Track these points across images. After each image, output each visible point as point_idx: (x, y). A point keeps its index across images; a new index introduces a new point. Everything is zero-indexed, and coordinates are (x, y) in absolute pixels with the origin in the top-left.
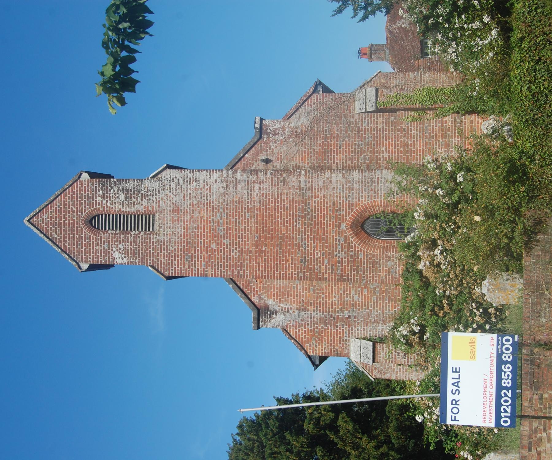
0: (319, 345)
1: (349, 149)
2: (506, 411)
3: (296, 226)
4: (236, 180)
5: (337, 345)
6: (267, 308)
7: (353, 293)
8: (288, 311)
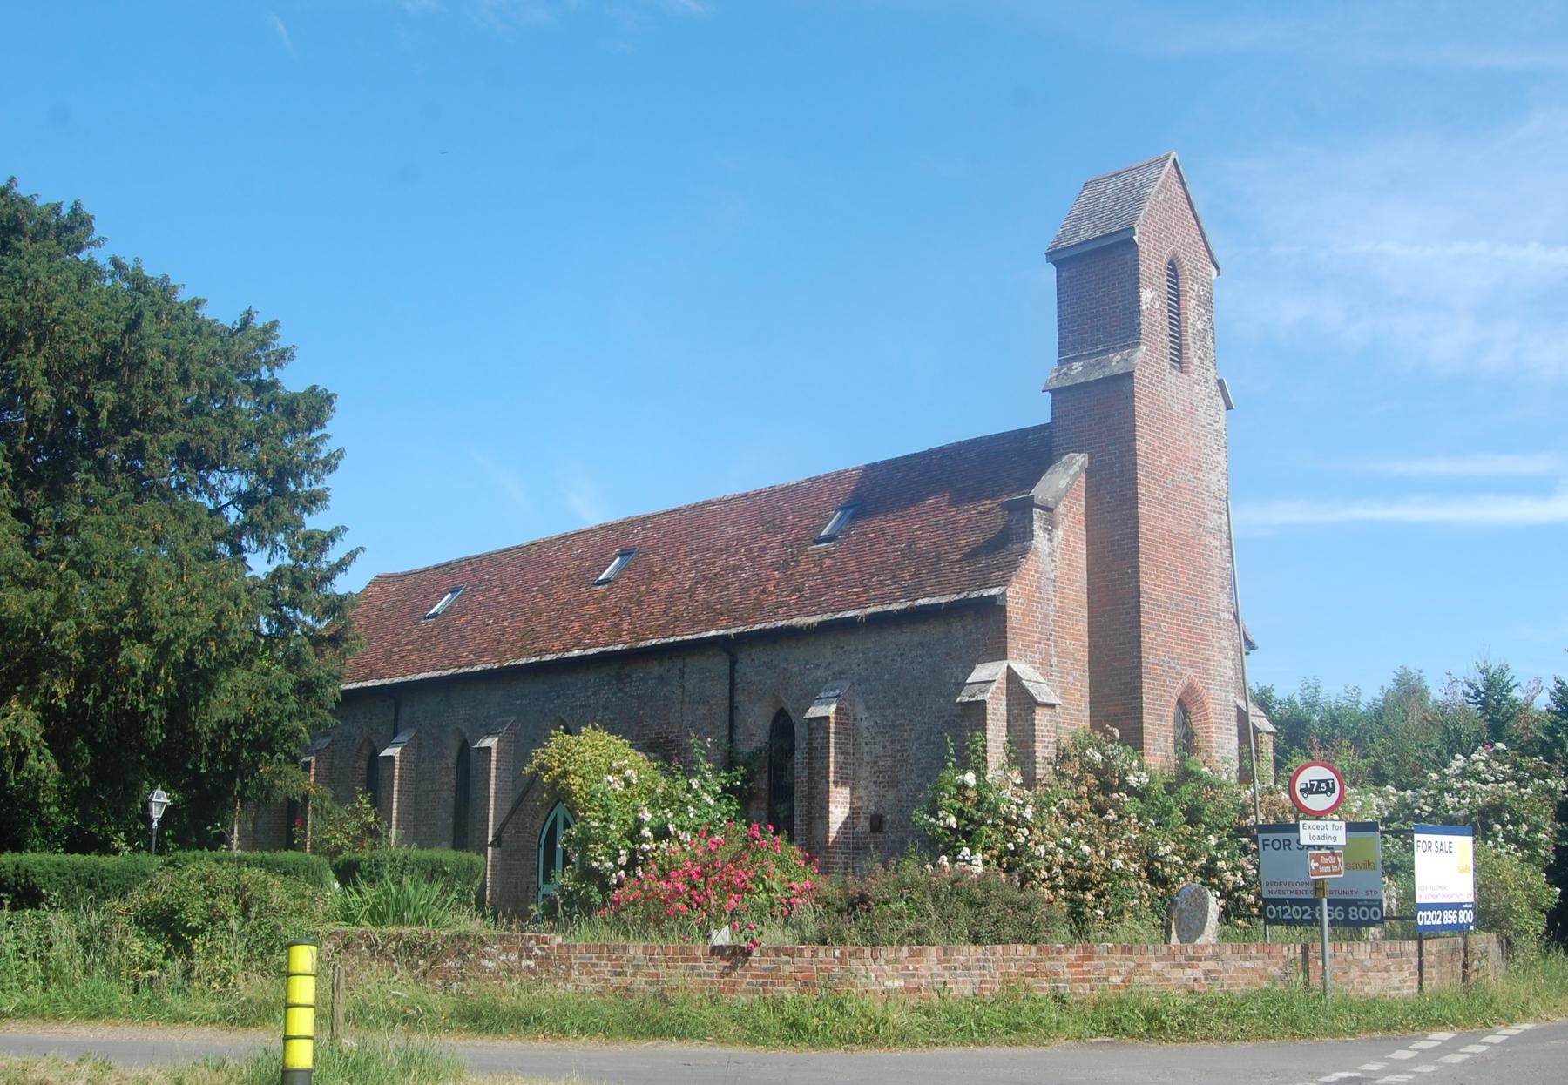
7: (1077, 674)
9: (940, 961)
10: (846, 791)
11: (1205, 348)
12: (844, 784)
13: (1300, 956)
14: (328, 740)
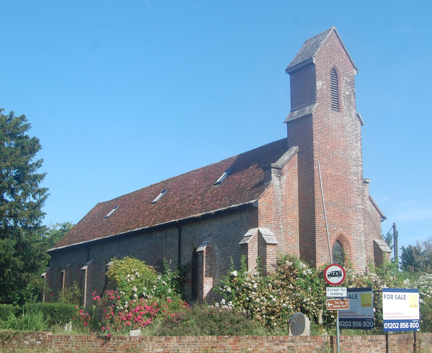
0: (264, 207)
2: (390, 325)
6: (282, 174)
7: (292, 232)
8: (281, 188)
9: (178, 342)
10: (211, 279)
11: (350, 103)
12: (210, 276)
13: (329, 341)
14: (70, 264)
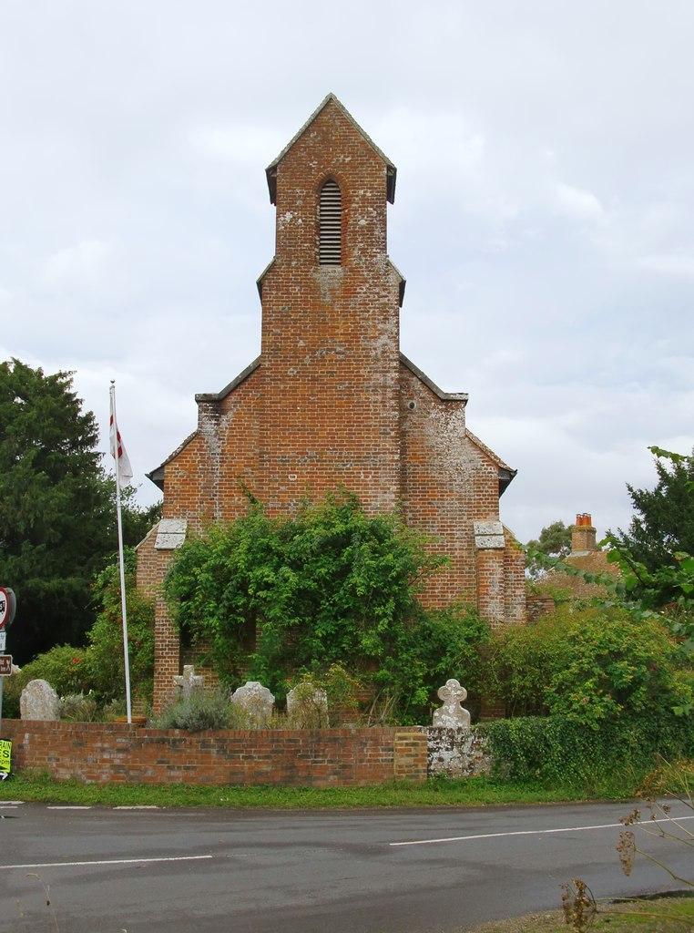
1: (428, 515)
3: (328, 449)
4: (387, 372)
5: (179, 503)
6: (223, 412)
